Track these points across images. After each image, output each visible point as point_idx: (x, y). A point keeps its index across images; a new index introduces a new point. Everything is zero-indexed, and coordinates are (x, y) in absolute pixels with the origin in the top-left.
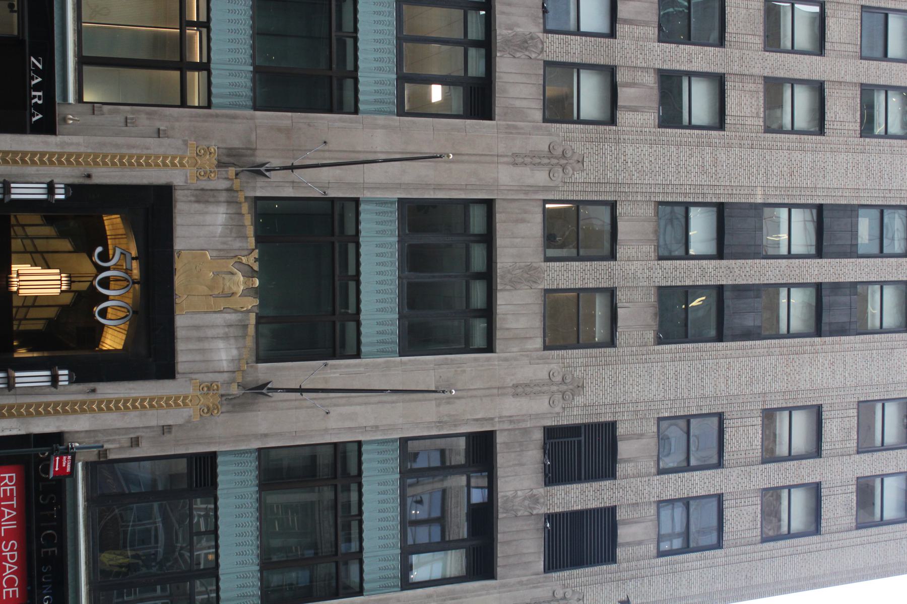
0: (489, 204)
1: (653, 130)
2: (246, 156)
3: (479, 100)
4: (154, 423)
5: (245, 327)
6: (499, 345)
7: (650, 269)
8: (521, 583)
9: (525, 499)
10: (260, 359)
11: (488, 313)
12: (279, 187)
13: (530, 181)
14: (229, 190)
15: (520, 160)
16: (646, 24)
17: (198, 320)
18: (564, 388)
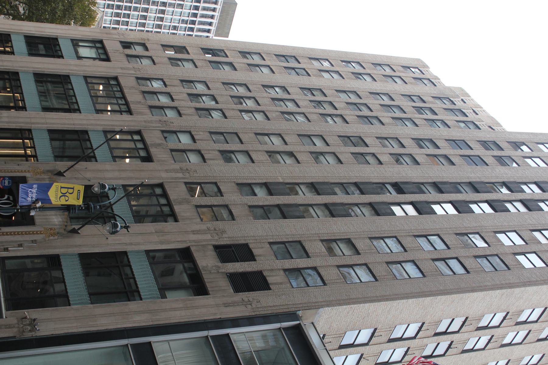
7: (241, 199)
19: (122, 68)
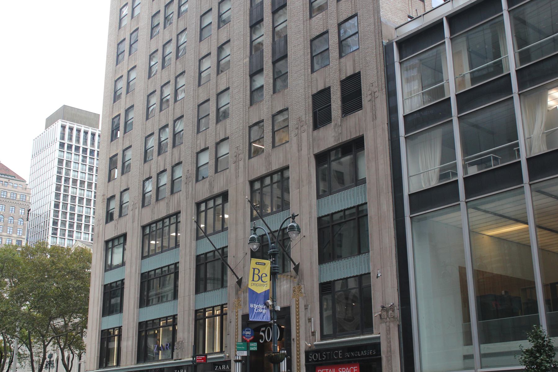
19: (133, 222)
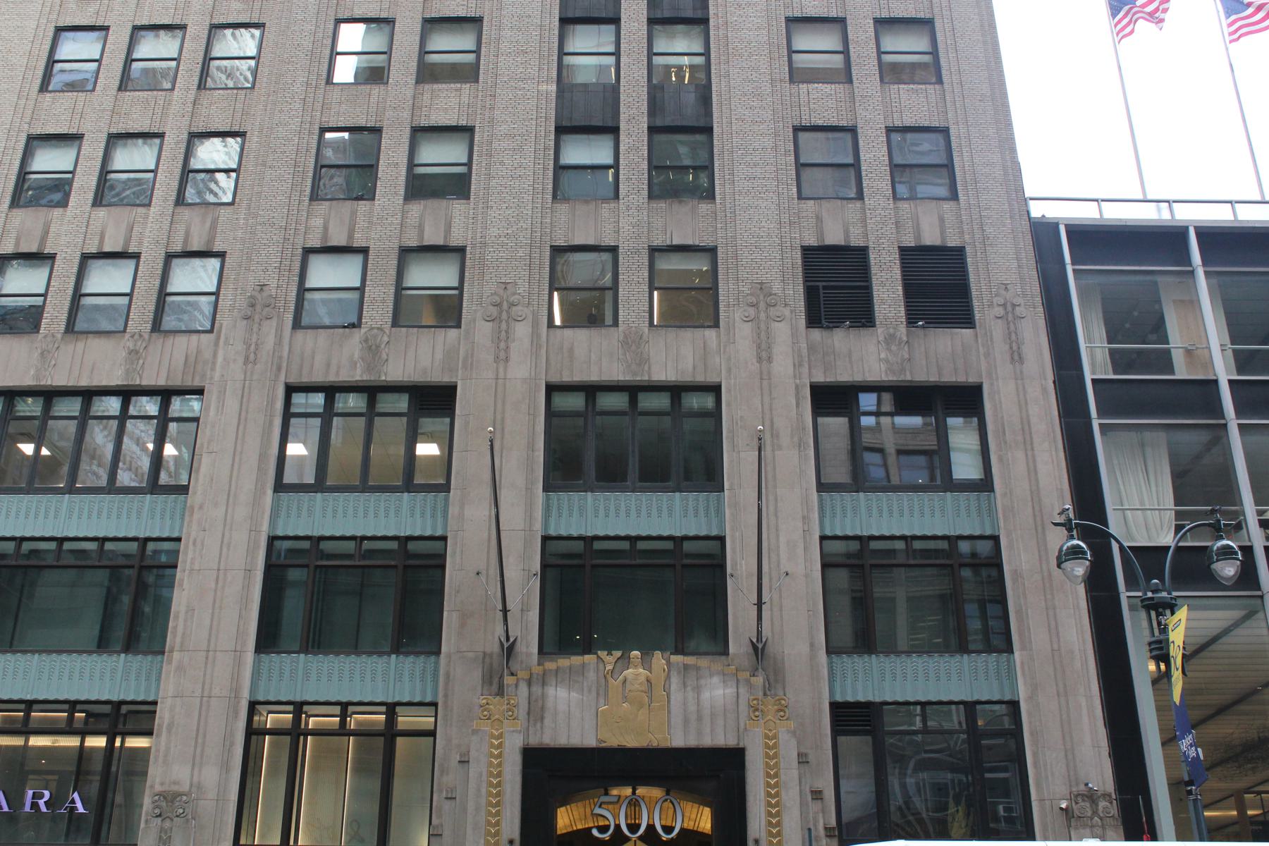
0: (551, 389)
1: (472, 205)
2: (491, 664)
3: (434, 400)
4: (795, 773)
5: (686, 667)
6: (712, 379)
7: (628, 208)
8: (987, 355)
9: (889, 349)
10: (722, 649)
11: (676, 391)
12: (527, 627)
13: (527, 342)
14: (529, 683)
15: (502, 355)
16: (354, 214)
17: (677, 719)
18: (762, 305)
